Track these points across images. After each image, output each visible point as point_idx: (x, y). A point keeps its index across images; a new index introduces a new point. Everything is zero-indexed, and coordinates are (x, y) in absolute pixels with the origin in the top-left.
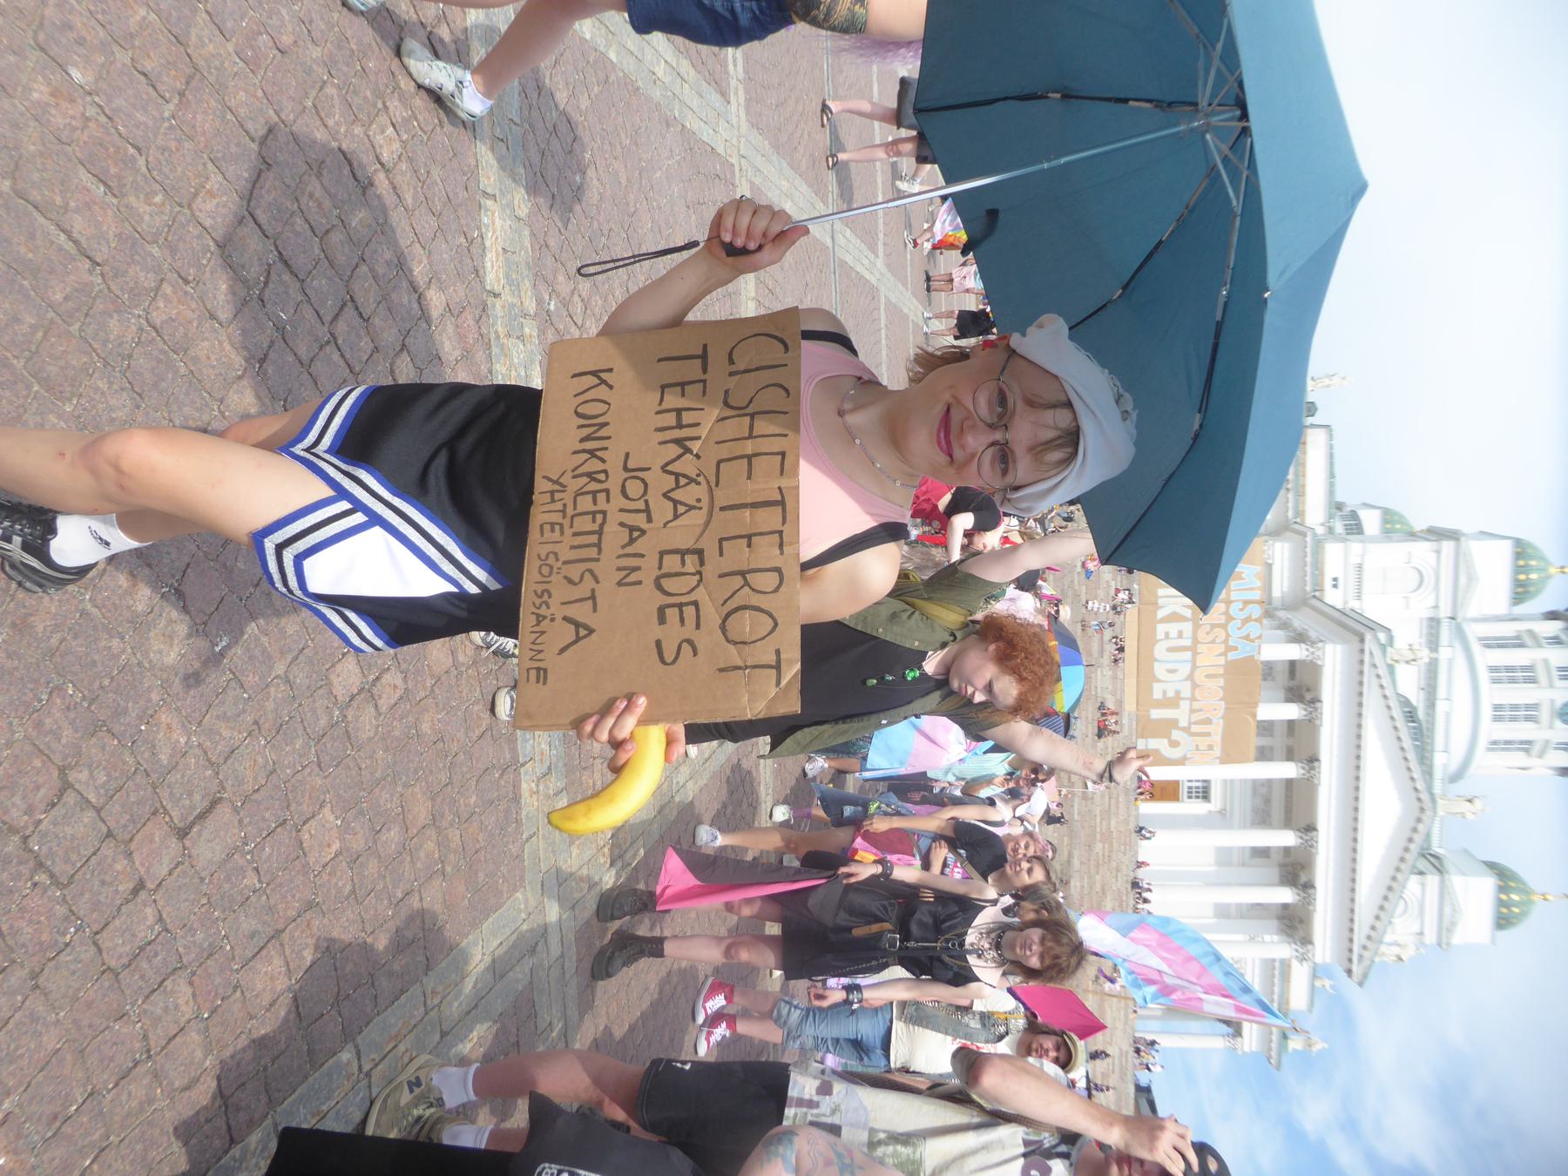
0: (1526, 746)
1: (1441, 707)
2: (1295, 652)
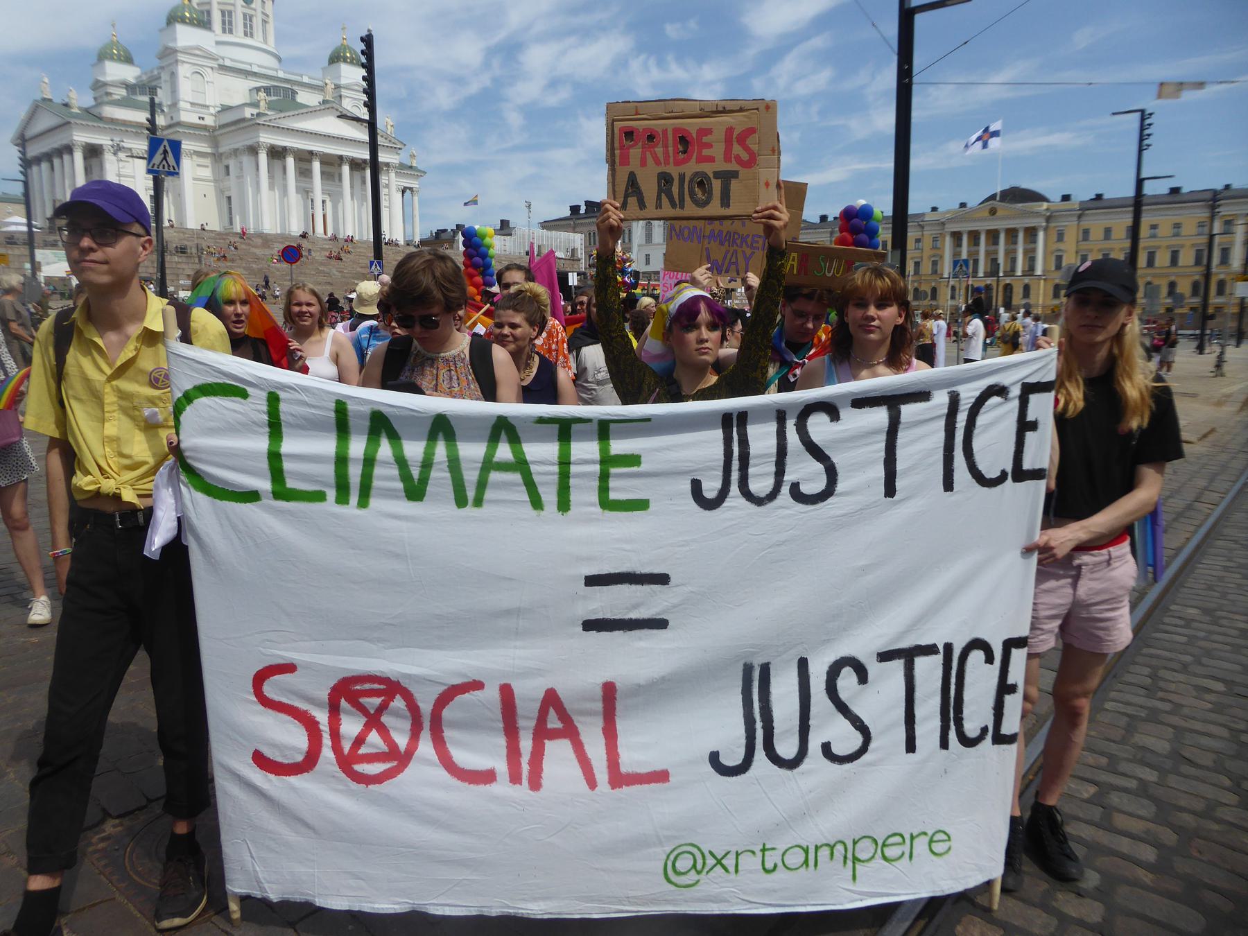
1: (255, 69)
2: (263, 157)
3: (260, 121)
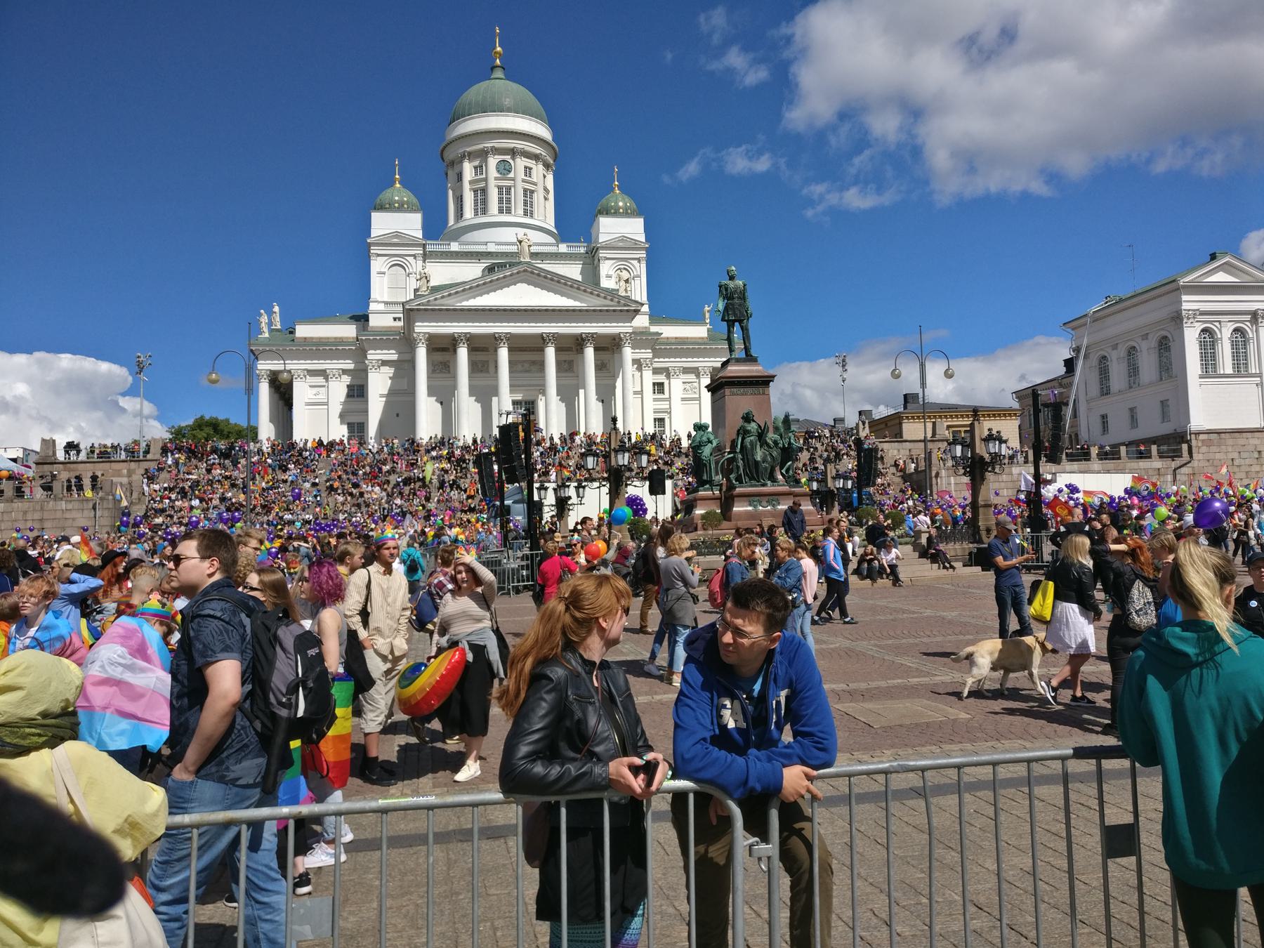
0: (528, 193)
1: (492, 248)
2: (421, 353)
3: (413, 306)
